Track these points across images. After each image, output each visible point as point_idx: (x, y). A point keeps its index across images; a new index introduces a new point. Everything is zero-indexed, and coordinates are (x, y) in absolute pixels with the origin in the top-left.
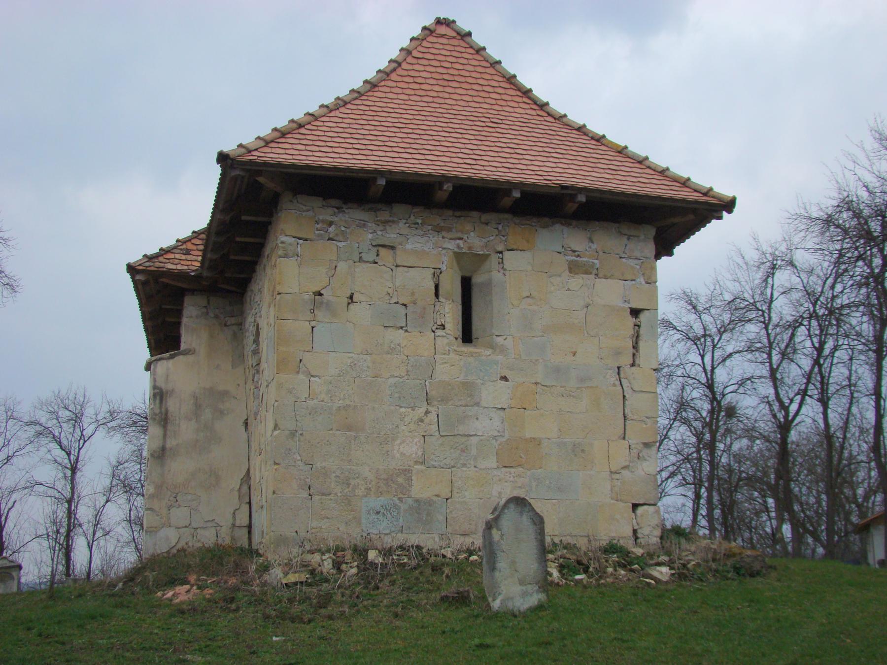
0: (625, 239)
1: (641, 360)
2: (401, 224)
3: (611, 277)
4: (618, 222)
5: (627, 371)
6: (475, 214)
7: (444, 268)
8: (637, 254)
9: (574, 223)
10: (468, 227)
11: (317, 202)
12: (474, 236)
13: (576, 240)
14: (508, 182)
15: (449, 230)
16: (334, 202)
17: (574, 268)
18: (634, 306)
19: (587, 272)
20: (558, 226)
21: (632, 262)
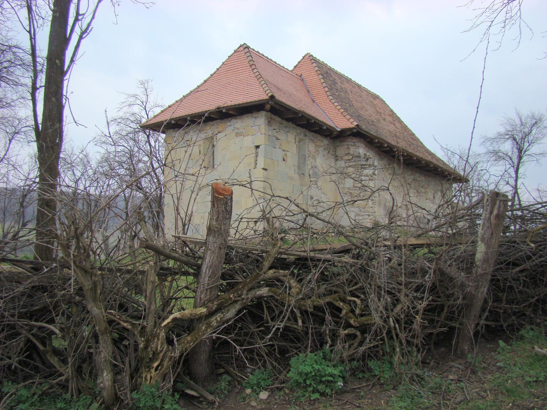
0: (254, 119)
1: (258, 166)
2: (192, 132)
3: (248, 135)
4: (252, 113)
5: (253, 170)
6: (210, 123)
7: (201, 144)
8: (258, 124)
9: (238, 117)
10: (208, 128)
11: (172, 130)
12: (210, 130)
13: (238, 124)
14: (202, 112)
15: (203, 130)
16: (176, 130)
17: (237, 135)
18: (256, 145)
19: (241, 135)
20: (233, 120)
21: (256, 128)
